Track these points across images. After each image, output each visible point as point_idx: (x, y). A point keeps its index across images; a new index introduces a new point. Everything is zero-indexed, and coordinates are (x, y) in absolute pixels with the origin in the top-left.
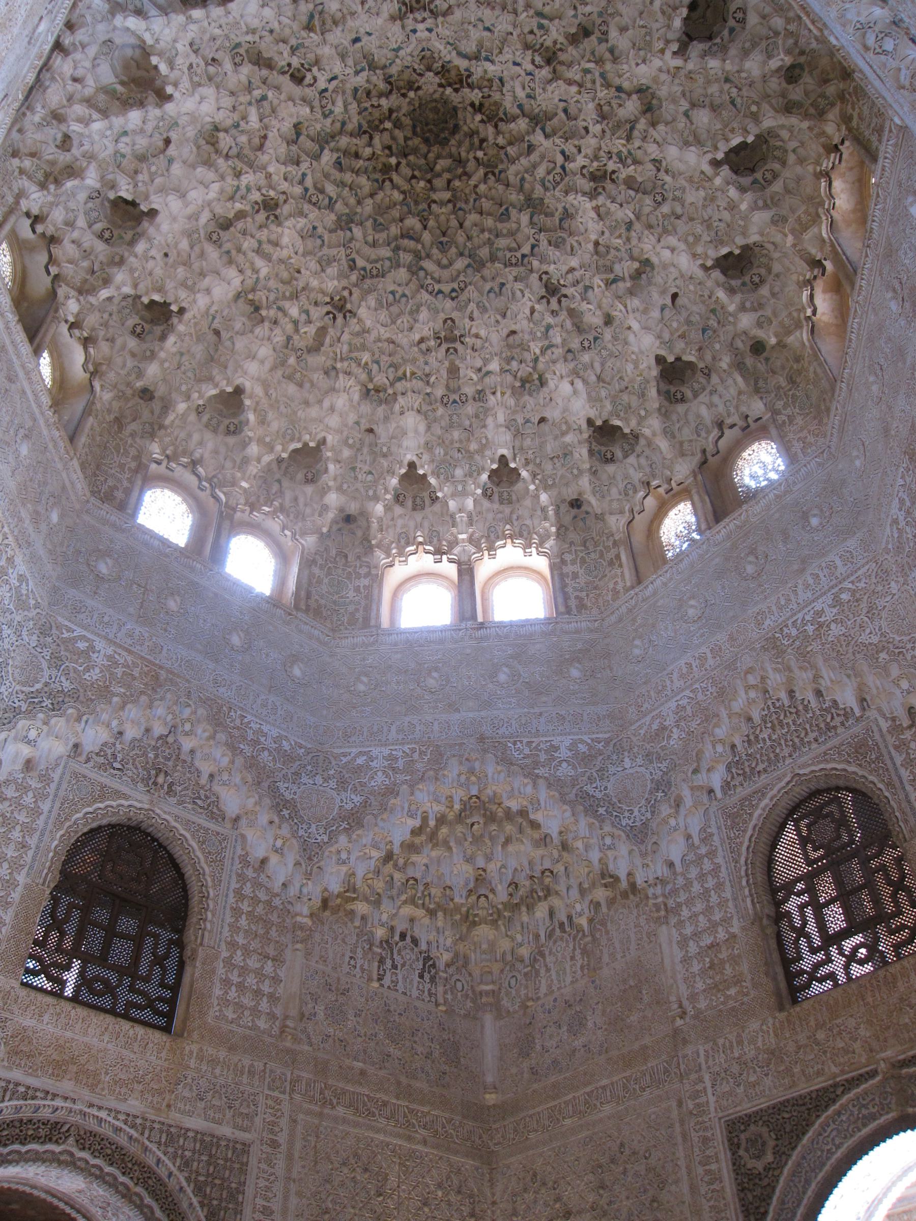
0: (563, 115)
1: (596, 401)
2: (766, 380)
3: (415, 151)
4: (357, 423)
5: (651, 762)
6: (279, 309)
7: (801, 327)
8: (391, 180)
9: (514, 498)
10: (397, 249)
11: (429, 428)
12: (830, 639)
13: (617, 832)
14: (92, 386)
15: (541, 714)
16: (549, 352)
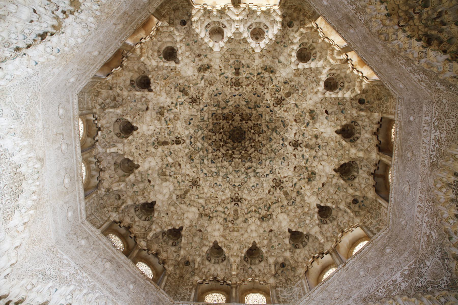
0: (258, 98)
1: (331, 162)
2: (372, 107)
3: (237, 146)
4: (265, 231)
5: (434, 253)
6: (216, 211)
7: (363, 81)
8: (234, 158)
9: (335, 217)
10: (247, 174)
11: (288, 215)
12: (444, 140)
13: (444, 292)
14: (165, 268)
15: (383, 274)
16: (308, 163)
